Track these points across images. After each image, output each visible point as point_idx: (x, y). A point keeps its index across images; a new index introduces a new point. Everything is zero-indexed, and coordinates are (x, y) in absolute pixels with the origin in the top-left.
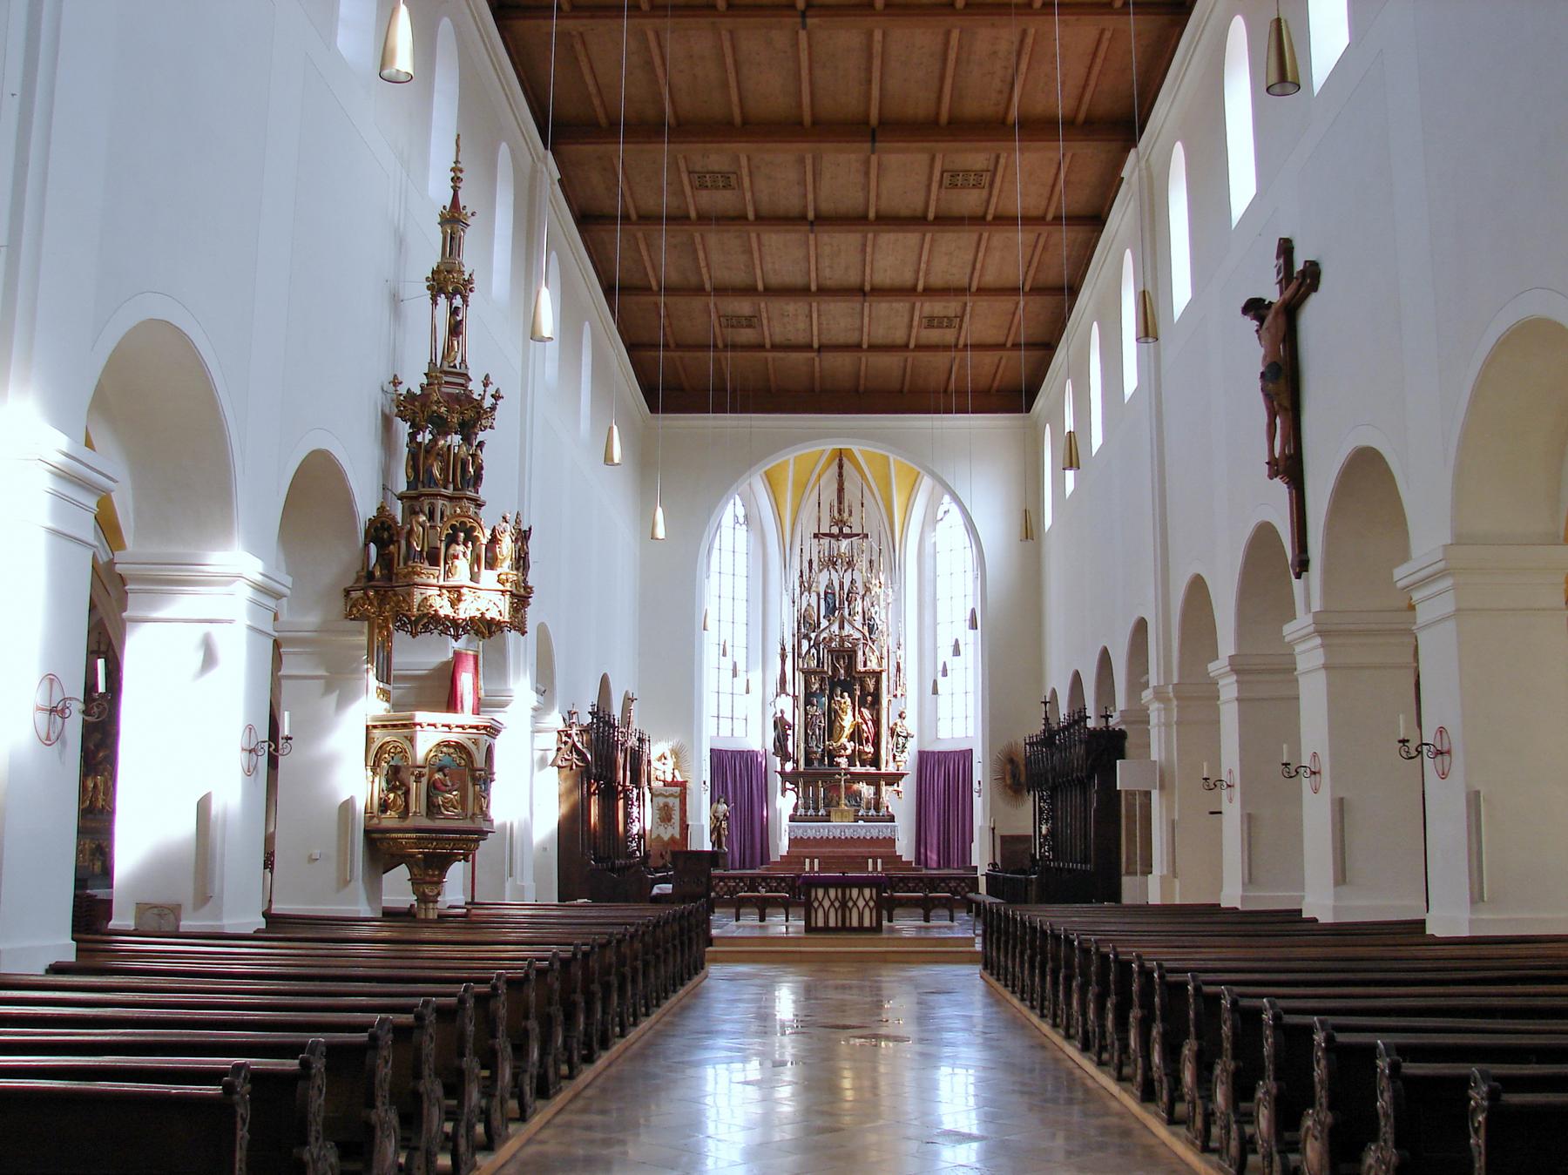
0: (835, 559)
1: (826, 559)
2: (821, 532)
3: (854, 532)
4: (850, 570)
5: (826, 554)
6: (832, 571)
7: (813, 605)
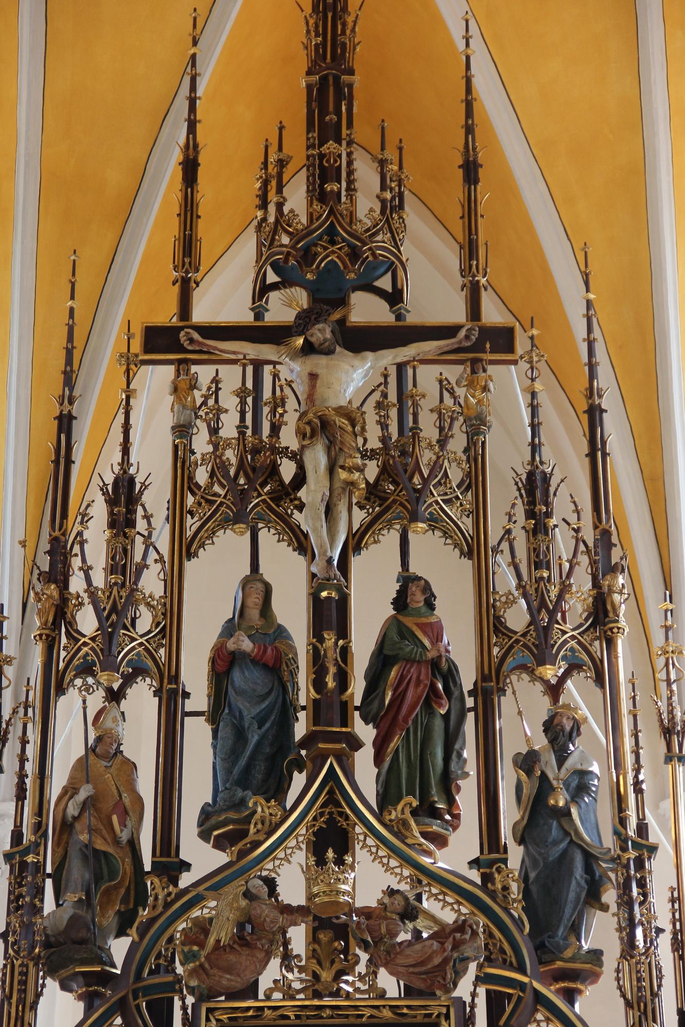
0: (287, 470)
1: (230, 455)
2: (200, 314)
3: (412, 319)
4: (390, 539)
5: (229, 430)
6: (267, 537)
7: (128, 751)
